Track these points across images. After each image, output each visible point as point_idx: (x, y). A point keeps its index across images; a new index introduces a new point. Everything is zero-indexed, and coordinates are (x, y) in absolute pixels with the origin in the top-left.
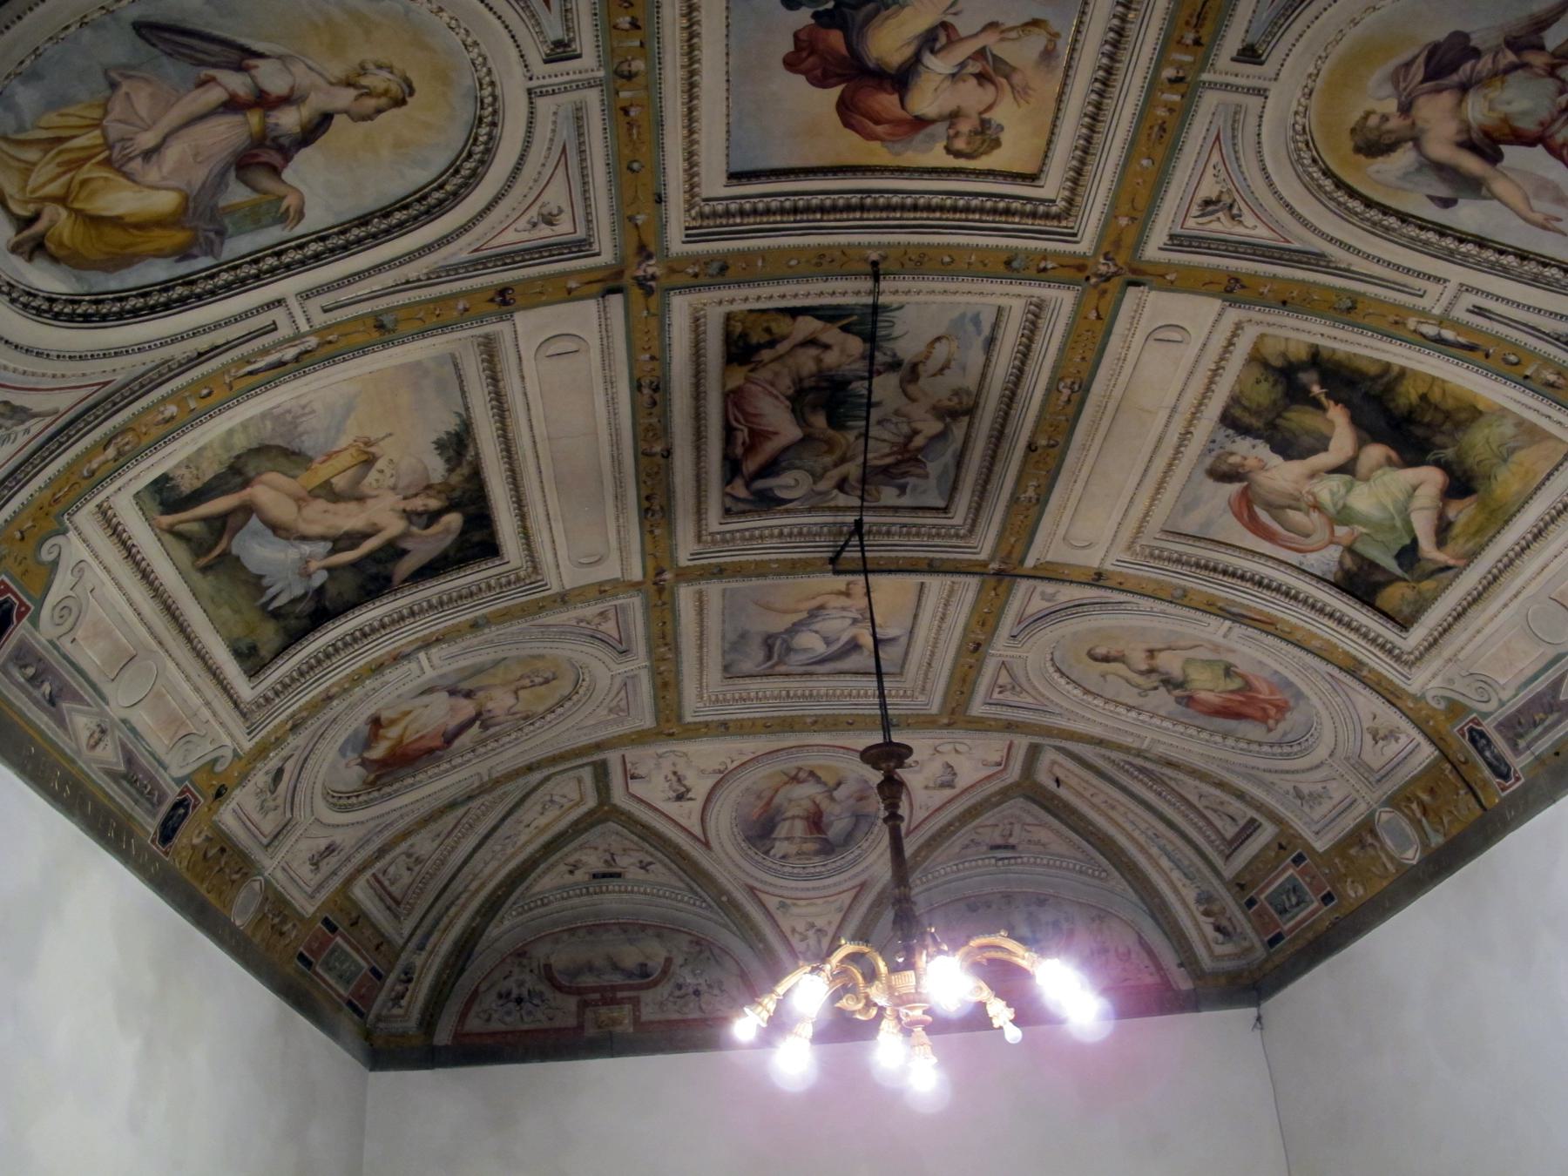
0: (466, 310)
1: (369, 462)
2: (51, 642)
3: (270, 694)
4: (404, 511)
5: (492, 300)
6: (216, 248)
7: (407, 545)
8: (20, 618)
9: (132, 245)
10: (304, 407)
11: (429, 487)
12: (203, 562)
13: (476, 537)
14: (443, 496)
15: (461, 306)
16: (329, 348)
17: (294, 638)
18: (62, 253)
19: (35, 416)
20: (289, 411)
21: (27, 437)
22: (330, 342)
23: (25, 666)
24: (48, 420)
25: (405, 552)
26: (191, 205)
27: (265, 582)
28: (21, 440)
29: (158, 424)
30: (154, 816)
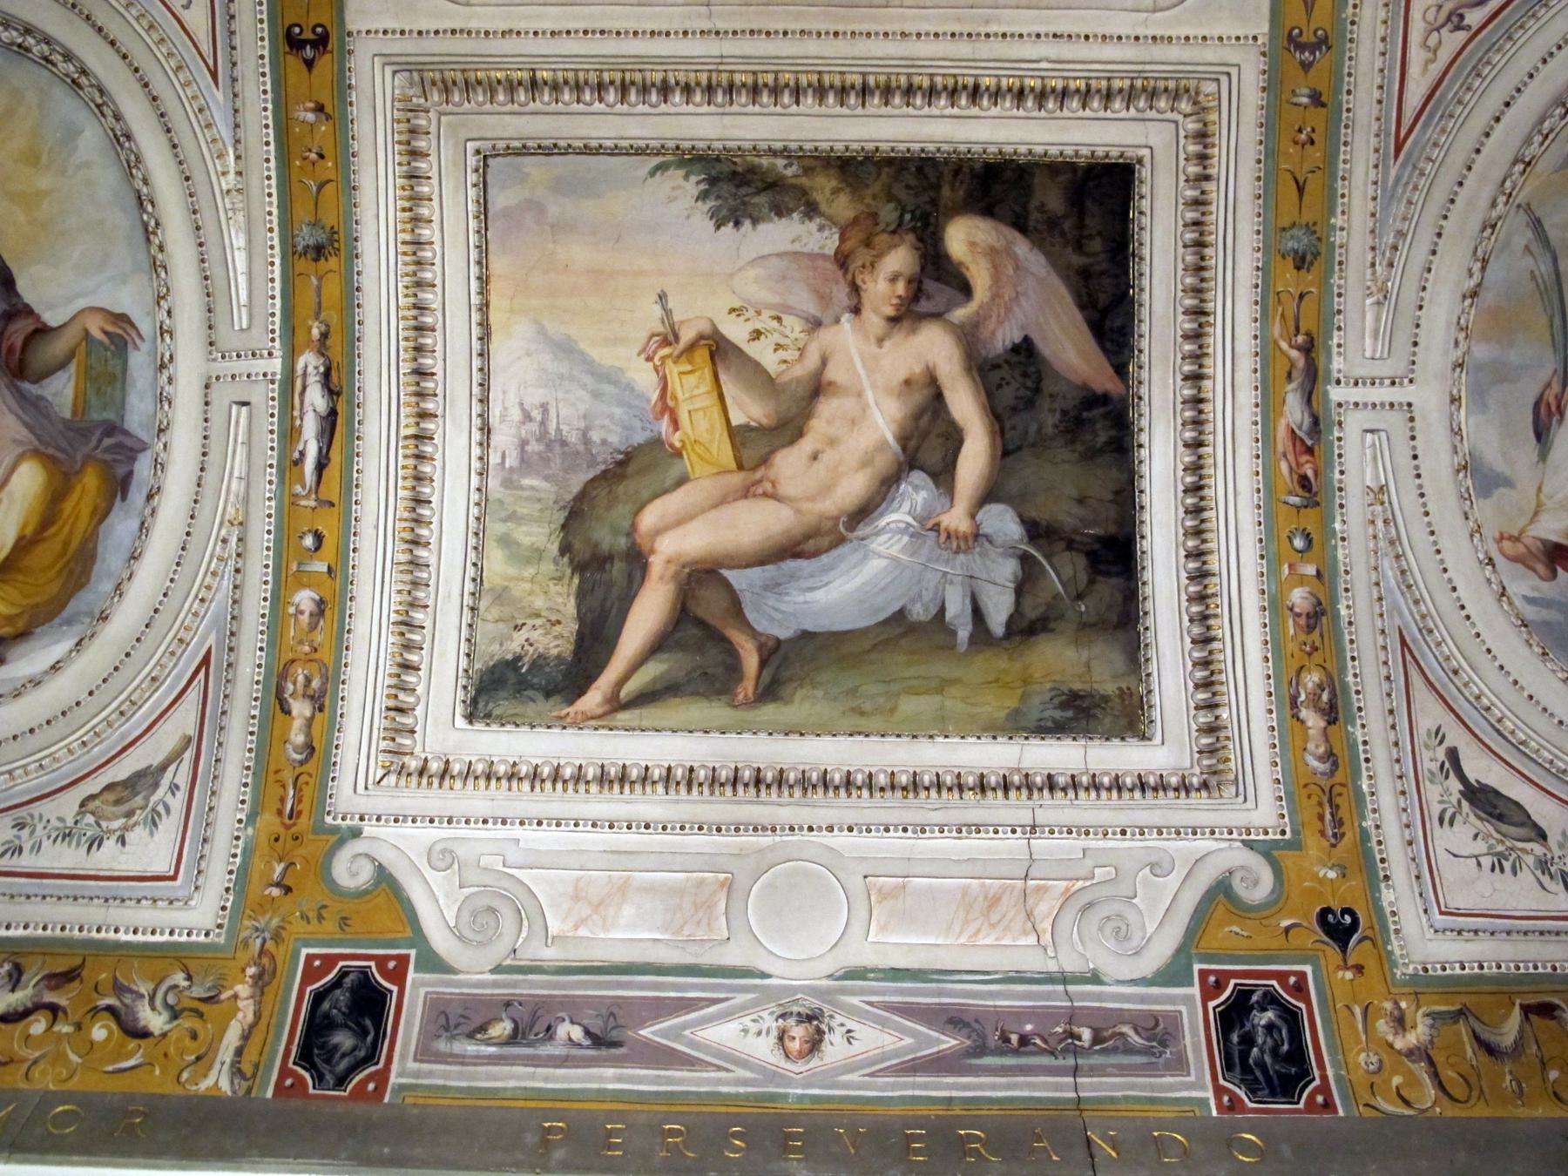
0: (320, 109)
1: (717, 349)
2: (497, 969)
3: (1205, 718)
4: (894, 320)
5: (309, 64)
6: (128, 442)
7: (1003, 336)
8: (399, 976)
9: (66, 544)
10: (527, 417)
11: (842, 260)
12: (747, 688)
13: (1051, 198)
14: (882, 239)
15: (311, 117)
16: (334, 341)
17: (1125, 620)
18: (21, 625)
19: (163, 768)
20: (523, 443)
21: (182, 795)
22: (325, 336)
23: (483, 1028)
24: (188, 755)
25: (1025, 350)
26: (51, 451)
27: (919, 613)
28: (177, 803)
29: (313, 627)
30: (1179, 1065)
